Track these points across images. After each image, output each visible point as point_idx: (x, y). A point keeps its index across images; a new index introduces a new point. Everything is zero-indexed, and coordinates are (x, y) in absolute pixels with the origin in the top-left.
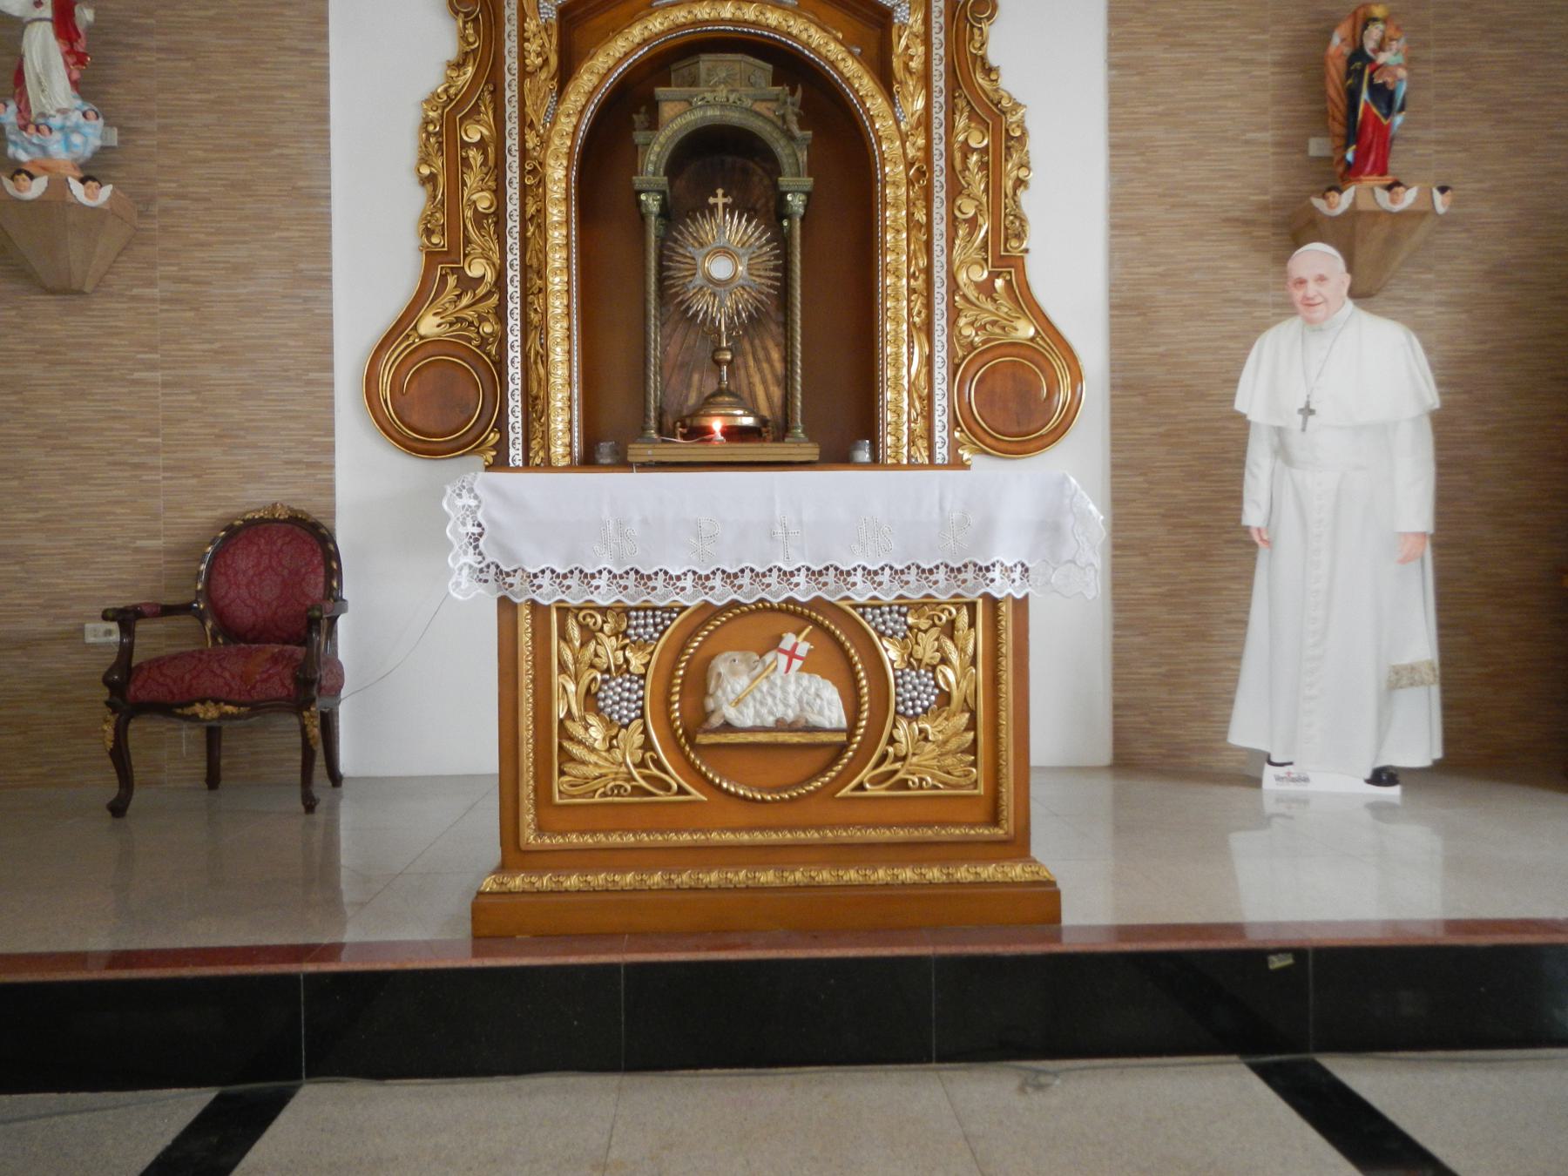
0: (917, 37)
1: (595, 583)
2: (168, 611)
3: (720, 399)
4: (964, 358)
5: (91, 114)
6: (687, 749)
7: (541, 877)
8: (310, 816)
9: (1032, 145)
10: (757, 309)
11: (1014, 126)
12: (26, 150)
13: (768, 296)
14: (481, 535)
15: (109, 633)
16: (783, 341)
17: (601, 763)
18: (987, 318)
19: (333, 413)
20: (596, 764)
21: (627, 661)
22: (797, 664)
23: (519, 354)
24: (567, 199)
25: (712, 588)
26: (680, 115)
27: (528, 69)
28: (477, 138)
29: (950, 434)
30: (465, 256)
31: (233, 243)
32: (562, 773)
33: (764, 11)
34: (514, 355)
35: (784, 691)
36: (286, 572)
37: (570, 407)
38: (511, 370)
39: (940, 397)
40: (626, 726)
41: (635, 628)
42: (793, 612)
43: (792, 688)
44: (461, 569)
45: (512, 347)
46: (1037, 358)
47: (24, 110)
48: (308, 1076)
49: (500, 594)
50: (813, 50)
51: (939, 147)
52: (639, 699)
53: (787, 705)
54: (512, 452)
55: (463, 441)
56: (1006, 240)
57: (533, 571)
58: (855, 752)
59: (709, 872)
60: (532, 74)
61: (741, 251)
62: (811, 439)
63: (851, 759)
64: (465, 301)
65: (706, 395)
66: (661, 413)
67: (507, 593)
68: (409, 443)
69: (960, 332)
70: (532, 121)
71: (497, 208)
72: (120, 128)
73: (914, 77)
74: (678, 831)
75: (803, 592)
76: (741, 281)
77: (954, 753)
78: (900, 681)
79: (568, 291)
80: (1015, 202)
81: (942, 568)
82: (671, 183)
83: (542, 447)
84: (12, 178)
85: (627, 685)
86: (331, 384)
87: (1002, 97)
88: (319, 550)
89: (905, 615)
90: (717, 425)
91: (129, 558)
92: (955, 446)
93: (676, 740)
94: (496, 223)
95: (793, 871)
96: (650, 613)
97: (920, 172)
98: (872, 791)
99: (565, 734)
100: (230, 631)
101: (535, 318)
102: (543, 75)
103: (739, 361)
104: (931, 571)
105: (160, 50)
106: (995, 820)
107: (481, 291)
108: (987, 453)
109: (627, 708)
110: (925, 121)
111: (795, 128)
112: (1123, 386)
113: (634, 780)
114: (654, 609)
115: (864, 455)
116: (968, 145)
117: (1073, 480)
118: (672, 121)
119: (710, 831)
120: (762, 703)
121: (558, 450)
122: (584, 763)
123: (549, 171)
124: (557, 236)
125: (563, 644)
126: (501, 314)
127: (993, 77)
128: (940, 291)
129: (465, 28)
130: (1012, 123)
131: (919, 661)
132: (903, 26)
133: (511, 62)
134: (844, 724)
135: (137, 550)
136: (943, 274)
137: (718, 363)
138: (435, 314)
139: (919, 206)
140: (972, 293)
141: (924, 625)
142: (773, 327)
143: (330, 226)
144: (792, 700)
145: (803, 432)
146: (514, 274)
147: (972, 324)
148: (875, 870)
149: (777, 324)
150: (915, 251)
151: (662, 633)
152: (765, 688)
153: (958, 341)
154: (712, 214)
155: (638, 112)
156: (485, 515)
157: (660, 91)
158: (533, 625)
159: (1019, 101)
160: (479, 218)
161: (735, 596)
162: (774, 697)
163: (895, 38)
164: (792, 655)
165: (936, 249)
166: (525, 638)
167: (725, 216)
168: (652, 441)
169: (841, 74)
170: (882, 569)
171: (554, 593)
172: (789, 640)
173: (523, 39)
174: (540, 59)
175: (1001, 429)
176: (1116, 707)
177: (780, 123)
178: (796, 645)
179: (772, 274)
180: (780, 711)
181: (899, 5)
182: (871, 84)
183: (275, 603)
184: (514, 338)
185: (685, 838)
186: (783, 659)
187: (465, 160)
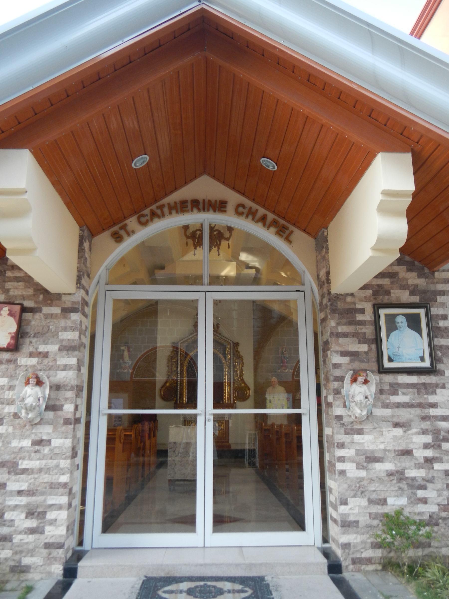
29: (233, 399)
34: (179, 389)
47: (123, 360)
92: (234, 401)
110: (230, 359)
112: (256, 391)
115: (221, 402)
140: (236, 380)
184: (179, 387)
187: (173, 364)
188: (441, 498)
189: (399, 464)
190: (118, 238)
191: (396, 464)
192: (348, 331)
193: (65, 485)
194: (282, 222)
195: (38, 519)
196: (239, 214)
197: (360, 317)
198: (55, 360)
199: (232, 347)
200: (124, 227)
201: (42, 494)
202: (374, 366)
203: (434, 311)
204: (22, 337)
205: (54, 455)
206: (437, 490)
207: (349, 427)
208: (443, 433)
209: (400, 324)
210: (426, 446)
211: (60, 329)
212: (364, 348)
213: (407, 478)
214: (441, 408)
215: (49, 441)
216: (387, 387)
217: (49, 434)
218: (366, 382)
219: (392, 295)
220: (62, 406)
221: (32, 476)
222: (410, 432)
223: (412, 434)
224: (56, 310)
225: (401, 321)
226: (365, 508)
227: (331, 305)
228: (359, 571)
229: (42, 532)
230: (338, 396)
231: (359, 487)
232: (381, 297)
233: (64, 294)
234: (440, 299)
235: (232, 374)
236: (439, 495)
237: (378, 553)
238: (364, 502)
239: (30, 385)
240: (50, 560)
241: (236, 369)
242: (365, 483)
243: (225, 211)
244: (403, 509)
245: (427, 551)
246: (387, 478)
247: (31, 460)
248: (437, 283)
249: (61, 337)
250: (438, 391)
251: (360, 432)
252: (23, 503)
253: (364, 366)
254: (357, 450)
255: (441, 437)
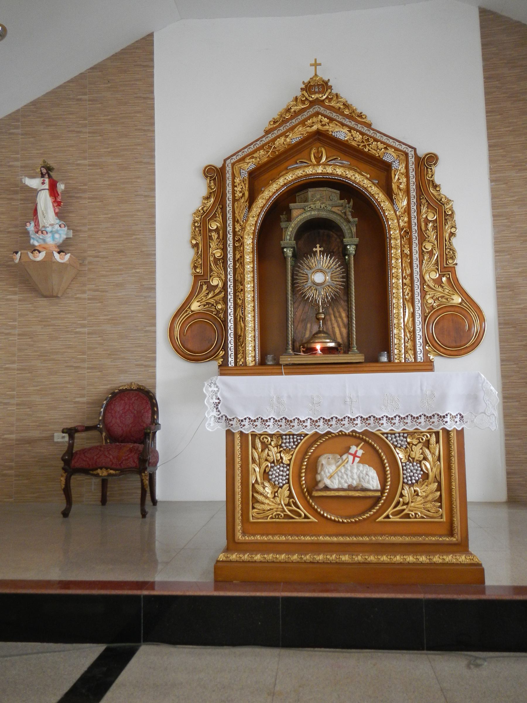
0: (403, 174)
1: (267, 424)
2: (88, 429)
3: (319, 335)
4: (429, 313)
5: (63, 226)
6: (309, 498)
7: (244, 555)
8: (144, 519)
9: (457, 217)
10: (335, 295)
11: (448, 210)
12: (37, 241)
13: (340, 289)
14: (219, 403)
15: (63, 437)
16: (347, 309)
17: (270, 503)
18: (438, 295)
19: (156, 344)
20: (268, 504)
21: (281, 458)
22: (357, 460)
23: (233, 318)
24: (253, 252)
25: (319, 426)
26: (300, 215)
27: (236, 198)
28: (215, 227)
30: (210, 276)
31: (117, 275)
32: (253, 508)
33: (335, 169)
34: (231, 318)
35: (352, 472)
36: (135, 412)
37: (255, 340)
38: (229, 325)
39: (418, 331)
40: (281, 487)
41: (285, 443)
42: (354, 436)
43: (355, 471)
44: (211, 418)
45: (230, 314)
46: (463, 312)
47: (37, 225)
48: (144, 641)
49: (227, 428)
50: (357, 184)
51: (414, 221)
52: (287, 475)
53: (353, 479)
54: (230, 359)
55: (209, 355)
56: (447, 260)
57: (241, 419)
58: (385, 500)
59: (319, 555)
60: (238, 200)
61: (328, 271)
62: (361, 353)
63: (383, 504)
64: (210, 295)
65: (313, 333)
66: (294, 341)
67: (230, 428)
68: (186, 356)
69: (427, 302)
70: (238, 219)
71: (223, 257)
72: (73, 230)
73: (402, 192)
74: (304, 536)
75: (360, 428)
76: (328, 283)
77: (431, 502)
78: (405, 468)
79: (253, 291)
80: (450, 243)
81: (423, 416)
82: (297, 243)
83: (243, 357)
84: (32, 253)
85: (282, 469)
86: (155, 332)
87: (442, 198)
88: (149, 402)
89: (406, 438)
90: (318, 347)
91: (72, 406)
92: (426, 353)
93: (304, 494)
94: (223, 263)
95: (357, 556)
96: (291, 437)
97: (406, 233)
98: (393, 519)
99: (255, 490)
100: (113, 438)
101: (239, 302)
102: (242, 200)
103: (328, 317)
104: (417, 418)
105: (89, 198)
106: (451, 533)
107: (217, 291)
108: (441, 356)
109: (282, 479)
110: (408, 210)
111: (350, 217)
113: (285, 512)
114: (293, 435)
115: (384, 359)
116: (428, 219)
117: (482, 375)
118: (297, 217)
119: (319, 536)
120: (342, 478)
121: (250, 360)
122: (263, 503)
123: (245, 240)
124: (248, 267)
125: (254, 450)
126: (225, 300)
127: (438, 189)
128: (417, 284)
129: (210, 183)
130: (447, 208)
131: (413, 459)
132: (397, 170)
133: (229, 196)
134: (379, 487)
135: (75, 403)
136: (418, 277)
137: (318, 319)
138: (198, 301)
139: (406, 247)
140: (432, 284)
141: (415, 442)
142: (342, 302)
143: (155, 266)
144: (355, 477)
145: (357, 349)
146: (230, 284)
147: (432, 298)
148: (395, 556)
149: (344, 301)
150: (405, 267)
151: (297, 446)
152: (343, 471)
153: (426, 305)
154: (315, 255)
155: (282, 214)
156: (221, 394)
157: (292, 205)
158: (241, 442)
159: (450, 198)
160: (216, 260)
161: (329, 430)
162: (347, 475)
163: (393, 176)
164: (355, 456)
165: (415, 266)
166: (238, 448)
167: (320, 256)
168: (290, 355)
169: (370, 193)
170: (395, 417)
171: (250, 428)
172: (353, 449)
173: (234, 186)
174: (241, 194)
175: (448, 345)
176: (508, 473)
177: (344, 216)
178: (356, 451)
179: (342, 280)
180: (350, 481)
181: (394, 161)
182: (383, 196)
183: (131, 426)
184: (231, 311)
185: (308, 538)
186: (351, 458)
187: (210, 237)
199: (412, 167)
241: (429, 247)
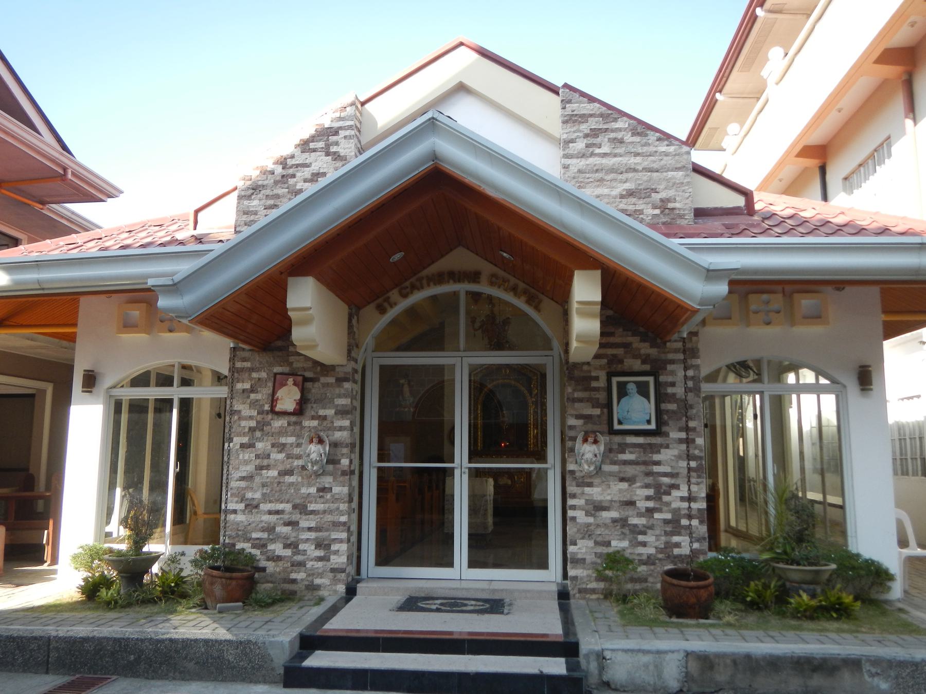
110: (537, 394)
188: (659, 542)
189: (623, 513)
190: (382, 310)
191: (620, 513)
192: (583, 396)
193: (344, 524)
194: (533, 291)
195: (324, 550)
196: (492, 284)
197: (594, 384)
198: (332, 422)
200: (387, 300)
201: (327, 530)
202: (605, 428)
203: (662, 378)
204: (305, 403)
205: (335, 500)
206: (656, 536)
207: (580, 480)
208: (664, 488)
209: (630, 391)
210: (648, 498)
211: (335, 396)
212: (597, 411)
213: (630, 525)
214: (664, 465)
215: (331, 489)
216: (615, 447)
217: (330, 483)
218: (596, 442)
219: (625, 364)
220: (340, 460)
221: (319, 516)
222: (634, 486)
223: (636, 488)
224: (331, 380)
225: (632, 388)
226: (592, 548)
227: (569, 373)
228: (585, 598)
229: (329, 560)
230: (571, 454)
231: (587, 531)
232: (615, 366)
233: (338, 365)
234: (670, 367)
235: (539, 414)
236: (657, 540)
237: (601, 585)
238: (591, 543)
239: (314, 443)
240: (335, 581)
242: (592, 528)
243: (479, 282)
244: (624, 550)
245: (644, 585)
246: (611, 524)
247: (317, 503)
248: (668, 352)
249: (336, 403)
250: (662, 450)
251: (590, 485)
252: (312, 537)
253: (596, 428)
254: (587, 500)
255: (662, 491)
